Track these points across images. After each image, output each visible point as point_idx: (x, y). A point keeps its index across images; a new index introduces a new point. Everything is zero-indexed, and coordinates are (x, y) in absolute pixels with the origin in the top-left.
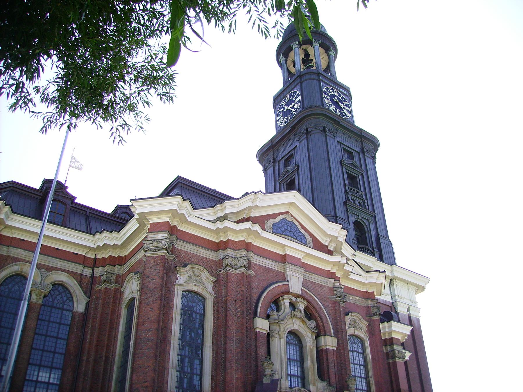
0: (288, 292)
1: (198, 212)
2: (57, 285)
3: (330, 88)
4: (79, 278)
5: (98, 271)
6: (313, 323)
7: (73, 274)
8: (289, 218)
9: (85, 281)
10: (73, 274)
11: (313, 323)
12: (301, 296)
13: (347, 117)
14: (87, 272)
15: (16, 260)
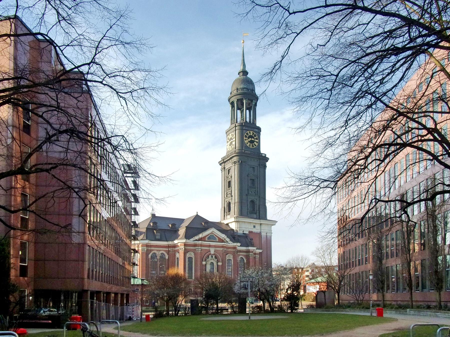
0: (211, 254)
1: (190, 240)
2: (162, 253)
3: (248, 132)
4: (165, 251)
5: (170, 249)
6: (216, 260)
7: (165, 251)
8: (212, 234)
9: (167, 251)
10: (165, 251)
11: (216, 260)
12: (214, 254)
13: (256, 145)
14: (167, 249)
15: (153, 250)
